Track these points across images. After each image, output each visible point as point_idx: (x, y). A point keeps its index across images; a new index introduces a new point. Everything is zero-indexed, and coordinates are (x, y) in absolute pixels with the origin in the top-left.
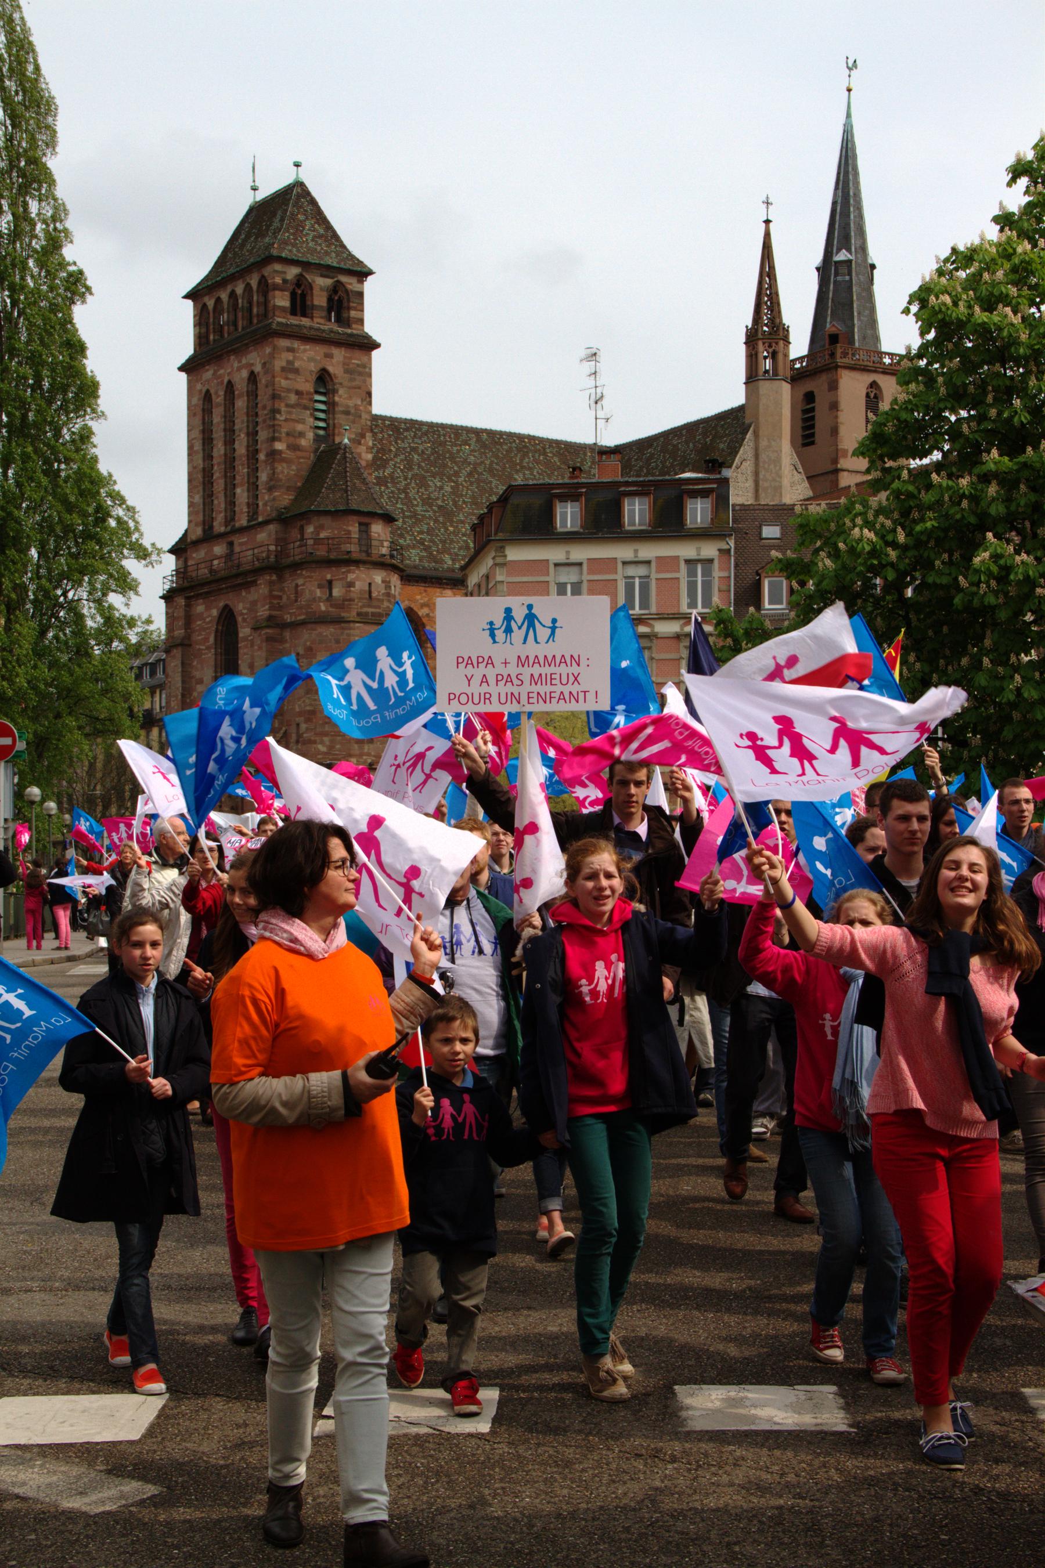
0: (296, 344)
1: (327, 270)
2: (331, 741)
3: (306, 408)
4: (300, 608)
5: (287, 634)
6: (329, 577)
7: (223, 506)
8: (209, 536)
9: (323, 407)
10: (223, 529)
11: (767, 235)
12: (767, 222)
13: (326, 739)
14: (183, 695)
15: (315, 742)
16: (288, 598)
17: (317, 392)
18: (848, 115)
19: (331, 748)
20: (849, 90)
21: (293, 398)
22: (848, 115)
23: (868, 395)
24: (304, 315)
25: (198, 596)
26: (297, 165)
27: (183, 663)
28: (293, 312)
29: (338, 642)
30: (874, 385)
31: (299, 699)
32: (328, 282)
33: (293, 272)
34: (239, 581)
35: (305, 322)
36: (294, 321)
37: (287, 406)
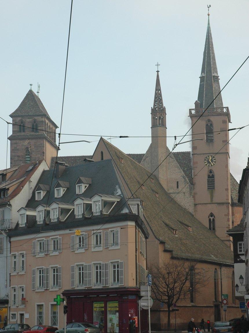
0: (18, 141)
1: (30, 116)
3: (21, 161)
9: (29, 159)
11: (158, 76)
12: (158, 72)
17: (26, 155)
21: (16, 158)
23: (207, 125)
24: (24, 131)
26: (31, 85)
28: (20, 131)
30: (209, 120)
32: (31, 120)
33: (19, 119)
35: (23, 134)
36: (19, 134)
37: (14, 161)
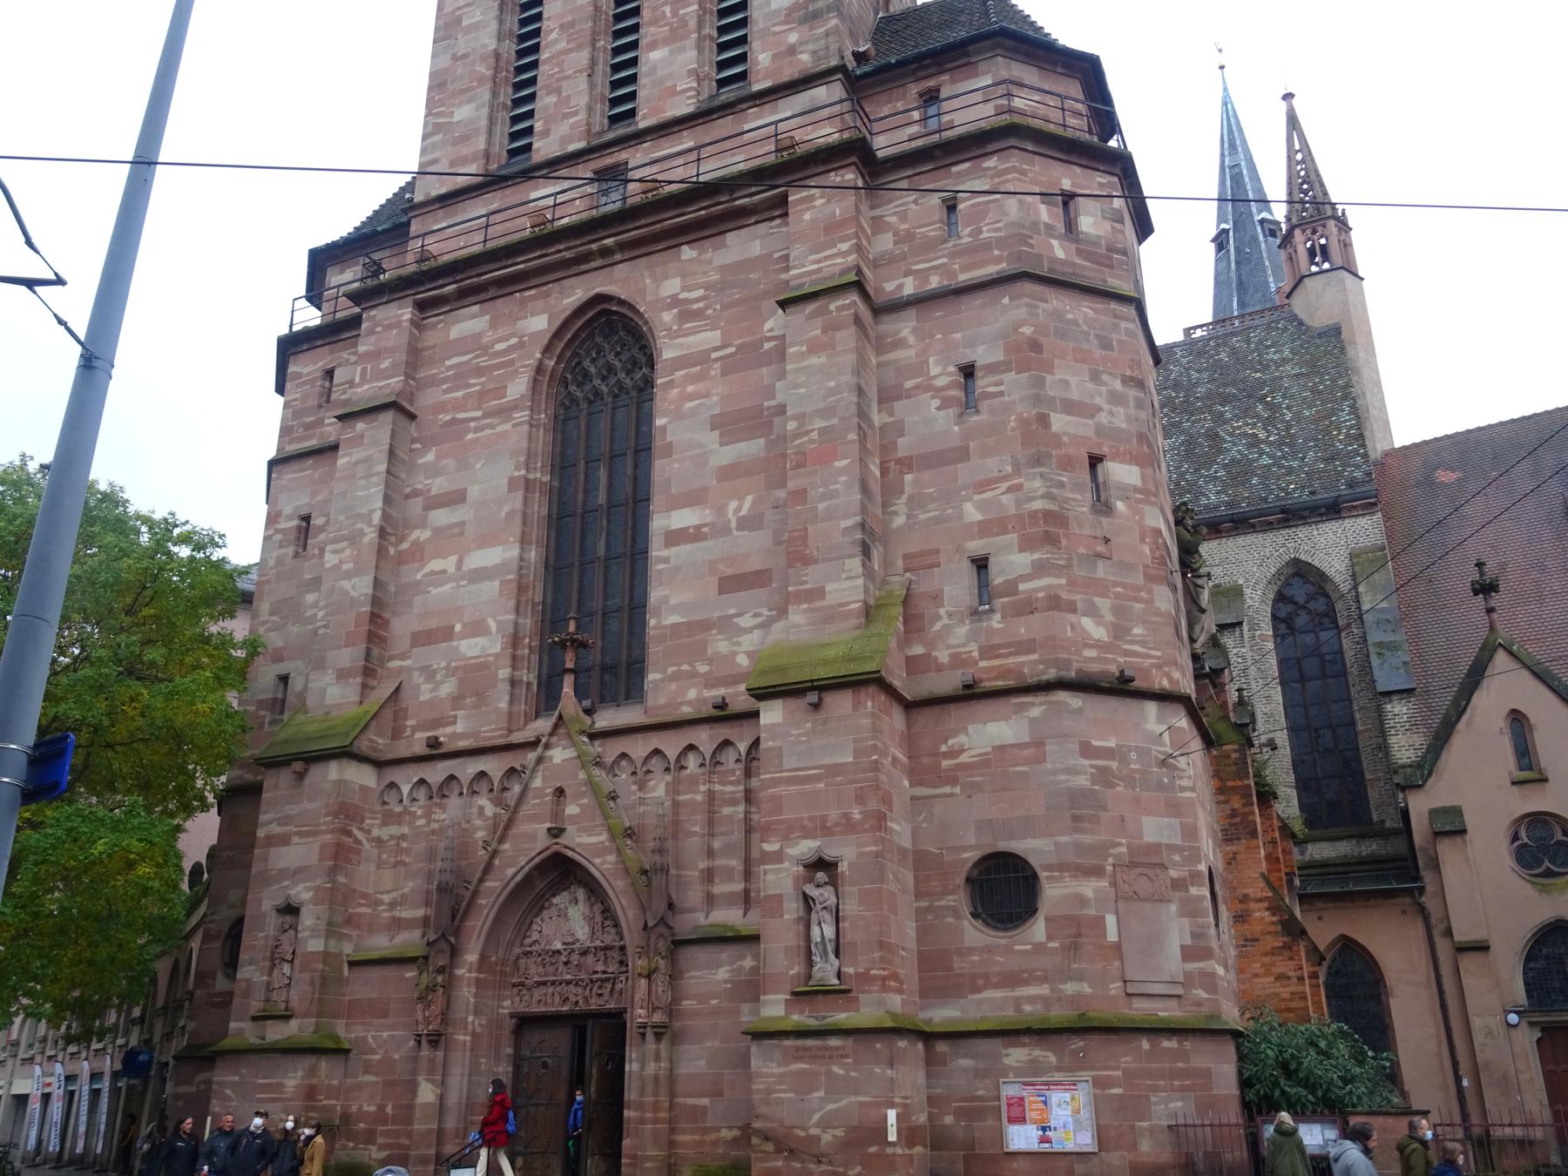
2: (1117, 610)
4: (987, 246)
5: (905, 326)
6: (1067, 185)
7: (584, 100)
8: (516, 166)
10: (582, 145)
12: (1288, 97)
13: (1103, 604)
14: (382, 533)
15: (1072, 608)
16: (903, 238)
18: (1225, 90)
19: (1119, 632)
20: (1222, 67)
22: (1225, 90)
25: (466, 295)
27: (392, 453)
29: (1106, 345)
31: (984, 485)
34: (692, 213)
